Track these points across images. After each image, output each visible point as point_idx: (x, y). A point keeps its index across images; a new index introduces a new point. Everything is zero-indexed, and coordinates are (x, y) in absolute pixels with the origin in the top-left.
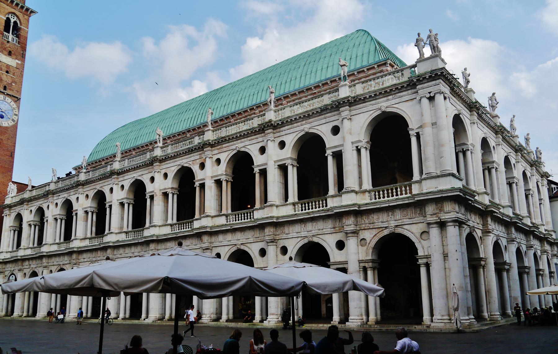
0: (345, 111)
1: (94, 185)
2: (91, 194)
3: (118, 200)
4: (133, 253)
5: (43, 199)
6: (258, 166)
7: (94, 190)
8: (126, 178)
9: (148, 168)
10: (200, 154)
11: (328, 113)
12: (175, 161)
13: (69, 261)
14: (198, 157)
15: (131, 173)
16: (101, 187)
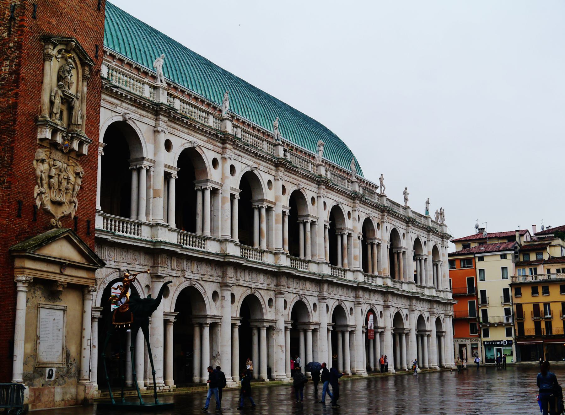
0: (432, 237)
1: (295, 179)
2: (291, 189)
3: (325, 221)
4: (340, 296)
5: (205, 139)
6: (404, 248)
7: (293, 185)
8: (329, 195)
9: (348, 199)
10: (379, 214)
11: (424, 231)
12: (365, 209)
13: (266, 285)
14: (377, 216)
15: (334, 193)
16: (303, 188)
